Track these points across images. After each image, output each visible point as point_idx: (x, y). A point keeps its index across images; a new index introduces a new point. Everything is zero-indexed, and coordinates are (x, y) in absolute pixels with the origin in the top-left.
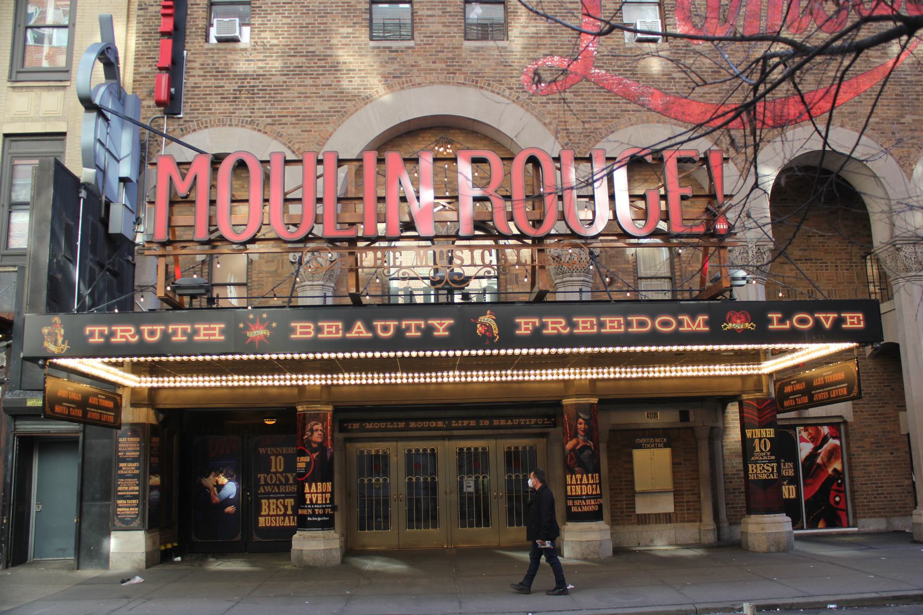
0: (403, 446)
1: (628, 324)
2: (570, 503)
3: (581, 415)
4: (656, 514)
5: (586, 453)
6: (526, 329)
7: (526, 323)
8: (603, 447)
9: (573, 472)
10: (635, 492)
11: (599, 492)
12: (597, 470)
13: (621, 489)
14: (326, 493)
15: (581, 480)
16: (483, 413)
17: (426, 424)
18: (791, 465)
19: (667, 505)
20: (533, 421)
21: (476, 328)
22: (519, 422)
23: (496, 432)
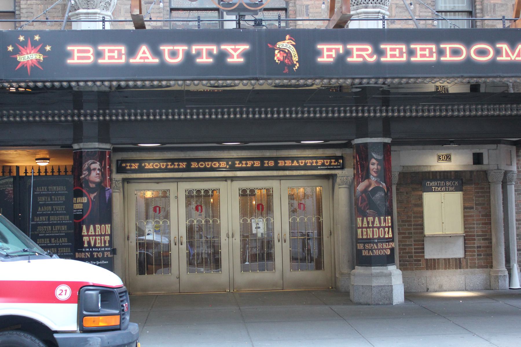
0: (185, 186)
1: (441, 52)
2: (360, 246)
3: (374, 155)
4: (445, 259)
6: (329, 56)
7: (329, 50)
8: (394, 188)
9: (364, 215)
10: (425, 236)
11: (391, 236)
12: (389, 213)
13: (409, 233)
14: (105, 235)
15: (373, 223)
16: (268, 154)
17: (208, 165)
20: (320, 162)
21: (274, 55)
22: (305, 164)
23: (281, 173)
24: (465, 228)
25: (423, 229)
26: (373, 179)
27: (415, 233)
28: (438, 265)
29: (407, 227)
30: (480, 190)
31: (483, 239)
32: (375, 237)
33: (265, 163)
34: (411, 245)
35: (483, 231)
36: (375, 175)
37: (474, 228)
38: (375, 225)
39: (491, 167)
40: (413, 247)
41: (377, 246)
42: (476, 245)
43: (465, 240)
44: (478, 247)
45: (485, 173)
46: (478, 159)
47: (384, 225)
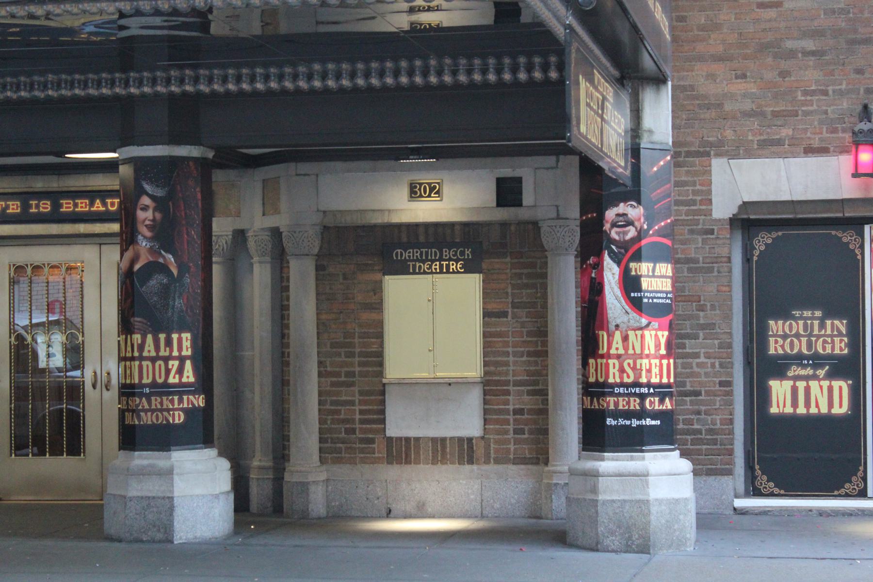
3: (148, 188)
4: (434, 440)
5: (156, 281)
13: (349, 374)
15: (141, 347)
16: (39, 184)
18: (842, 325)
19: (466, 421)
24: (486, 364)
25: (381, 364)
26: (143, 244)
27: (363, 375)
28: (417, 453)
29: (343, 358)
30: (525, 271)
31: (529, 393)
32: (145, 381)
33: (30, 206)
34: (352, 403)
35: (529, 373)
36: (148, 234)
37: (507, 364)
38: (145, 354)
39: (540, 214)
40: (357, 408)
41: (150, 403)
42: (511, 407)
43: (485, 393)
44: (516, 412)
45: (535, 225)
46: (508, 192)
47: (167, 354)
